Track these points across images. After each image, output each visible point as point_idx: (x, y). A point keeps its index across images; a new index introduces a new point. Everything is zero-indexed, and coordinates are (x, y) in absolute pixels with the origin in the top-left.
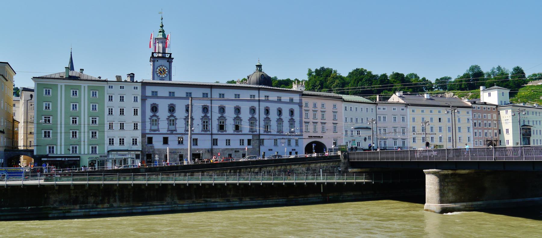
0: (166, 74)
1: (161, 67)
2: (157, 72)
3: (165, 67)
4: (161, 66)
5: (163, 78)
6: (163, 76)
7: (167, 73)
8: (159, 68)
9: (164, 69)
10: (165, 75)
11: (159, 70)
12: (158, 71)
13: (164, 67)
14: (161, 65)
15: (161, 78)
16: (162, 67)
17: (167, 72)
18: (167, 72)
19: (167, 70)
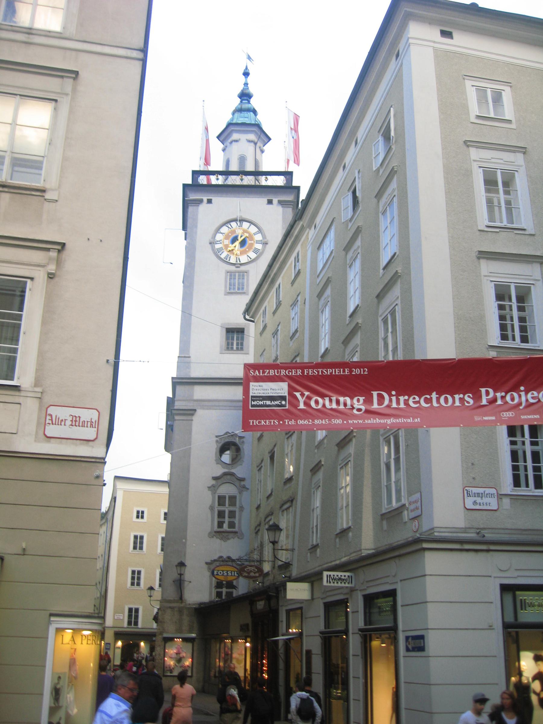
0: (256, 251)
1: (234, 224)
2: (217, 246)
3: (251, 223)
4: (235, 220)
5: (243, 268)
6: (244, 259)
7: (259, 246)
8: (225, 230)
9: (245, 231)
10: (253, 255)
11: (227, 238)
12: (220, 242)
13: (245, 225)
14: (234, 217)
15: (233, 268)
16: (241, 226)
17: (257, 242)
18: (257, 242)
19: (259, 237)
